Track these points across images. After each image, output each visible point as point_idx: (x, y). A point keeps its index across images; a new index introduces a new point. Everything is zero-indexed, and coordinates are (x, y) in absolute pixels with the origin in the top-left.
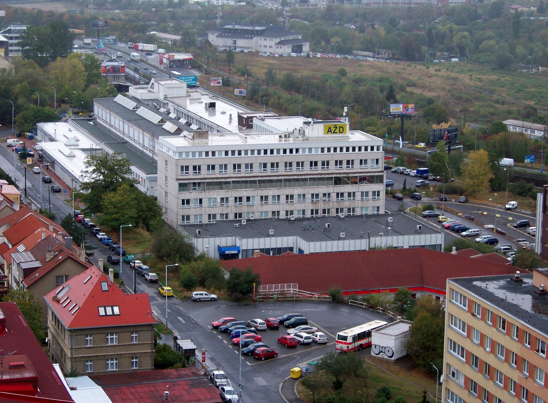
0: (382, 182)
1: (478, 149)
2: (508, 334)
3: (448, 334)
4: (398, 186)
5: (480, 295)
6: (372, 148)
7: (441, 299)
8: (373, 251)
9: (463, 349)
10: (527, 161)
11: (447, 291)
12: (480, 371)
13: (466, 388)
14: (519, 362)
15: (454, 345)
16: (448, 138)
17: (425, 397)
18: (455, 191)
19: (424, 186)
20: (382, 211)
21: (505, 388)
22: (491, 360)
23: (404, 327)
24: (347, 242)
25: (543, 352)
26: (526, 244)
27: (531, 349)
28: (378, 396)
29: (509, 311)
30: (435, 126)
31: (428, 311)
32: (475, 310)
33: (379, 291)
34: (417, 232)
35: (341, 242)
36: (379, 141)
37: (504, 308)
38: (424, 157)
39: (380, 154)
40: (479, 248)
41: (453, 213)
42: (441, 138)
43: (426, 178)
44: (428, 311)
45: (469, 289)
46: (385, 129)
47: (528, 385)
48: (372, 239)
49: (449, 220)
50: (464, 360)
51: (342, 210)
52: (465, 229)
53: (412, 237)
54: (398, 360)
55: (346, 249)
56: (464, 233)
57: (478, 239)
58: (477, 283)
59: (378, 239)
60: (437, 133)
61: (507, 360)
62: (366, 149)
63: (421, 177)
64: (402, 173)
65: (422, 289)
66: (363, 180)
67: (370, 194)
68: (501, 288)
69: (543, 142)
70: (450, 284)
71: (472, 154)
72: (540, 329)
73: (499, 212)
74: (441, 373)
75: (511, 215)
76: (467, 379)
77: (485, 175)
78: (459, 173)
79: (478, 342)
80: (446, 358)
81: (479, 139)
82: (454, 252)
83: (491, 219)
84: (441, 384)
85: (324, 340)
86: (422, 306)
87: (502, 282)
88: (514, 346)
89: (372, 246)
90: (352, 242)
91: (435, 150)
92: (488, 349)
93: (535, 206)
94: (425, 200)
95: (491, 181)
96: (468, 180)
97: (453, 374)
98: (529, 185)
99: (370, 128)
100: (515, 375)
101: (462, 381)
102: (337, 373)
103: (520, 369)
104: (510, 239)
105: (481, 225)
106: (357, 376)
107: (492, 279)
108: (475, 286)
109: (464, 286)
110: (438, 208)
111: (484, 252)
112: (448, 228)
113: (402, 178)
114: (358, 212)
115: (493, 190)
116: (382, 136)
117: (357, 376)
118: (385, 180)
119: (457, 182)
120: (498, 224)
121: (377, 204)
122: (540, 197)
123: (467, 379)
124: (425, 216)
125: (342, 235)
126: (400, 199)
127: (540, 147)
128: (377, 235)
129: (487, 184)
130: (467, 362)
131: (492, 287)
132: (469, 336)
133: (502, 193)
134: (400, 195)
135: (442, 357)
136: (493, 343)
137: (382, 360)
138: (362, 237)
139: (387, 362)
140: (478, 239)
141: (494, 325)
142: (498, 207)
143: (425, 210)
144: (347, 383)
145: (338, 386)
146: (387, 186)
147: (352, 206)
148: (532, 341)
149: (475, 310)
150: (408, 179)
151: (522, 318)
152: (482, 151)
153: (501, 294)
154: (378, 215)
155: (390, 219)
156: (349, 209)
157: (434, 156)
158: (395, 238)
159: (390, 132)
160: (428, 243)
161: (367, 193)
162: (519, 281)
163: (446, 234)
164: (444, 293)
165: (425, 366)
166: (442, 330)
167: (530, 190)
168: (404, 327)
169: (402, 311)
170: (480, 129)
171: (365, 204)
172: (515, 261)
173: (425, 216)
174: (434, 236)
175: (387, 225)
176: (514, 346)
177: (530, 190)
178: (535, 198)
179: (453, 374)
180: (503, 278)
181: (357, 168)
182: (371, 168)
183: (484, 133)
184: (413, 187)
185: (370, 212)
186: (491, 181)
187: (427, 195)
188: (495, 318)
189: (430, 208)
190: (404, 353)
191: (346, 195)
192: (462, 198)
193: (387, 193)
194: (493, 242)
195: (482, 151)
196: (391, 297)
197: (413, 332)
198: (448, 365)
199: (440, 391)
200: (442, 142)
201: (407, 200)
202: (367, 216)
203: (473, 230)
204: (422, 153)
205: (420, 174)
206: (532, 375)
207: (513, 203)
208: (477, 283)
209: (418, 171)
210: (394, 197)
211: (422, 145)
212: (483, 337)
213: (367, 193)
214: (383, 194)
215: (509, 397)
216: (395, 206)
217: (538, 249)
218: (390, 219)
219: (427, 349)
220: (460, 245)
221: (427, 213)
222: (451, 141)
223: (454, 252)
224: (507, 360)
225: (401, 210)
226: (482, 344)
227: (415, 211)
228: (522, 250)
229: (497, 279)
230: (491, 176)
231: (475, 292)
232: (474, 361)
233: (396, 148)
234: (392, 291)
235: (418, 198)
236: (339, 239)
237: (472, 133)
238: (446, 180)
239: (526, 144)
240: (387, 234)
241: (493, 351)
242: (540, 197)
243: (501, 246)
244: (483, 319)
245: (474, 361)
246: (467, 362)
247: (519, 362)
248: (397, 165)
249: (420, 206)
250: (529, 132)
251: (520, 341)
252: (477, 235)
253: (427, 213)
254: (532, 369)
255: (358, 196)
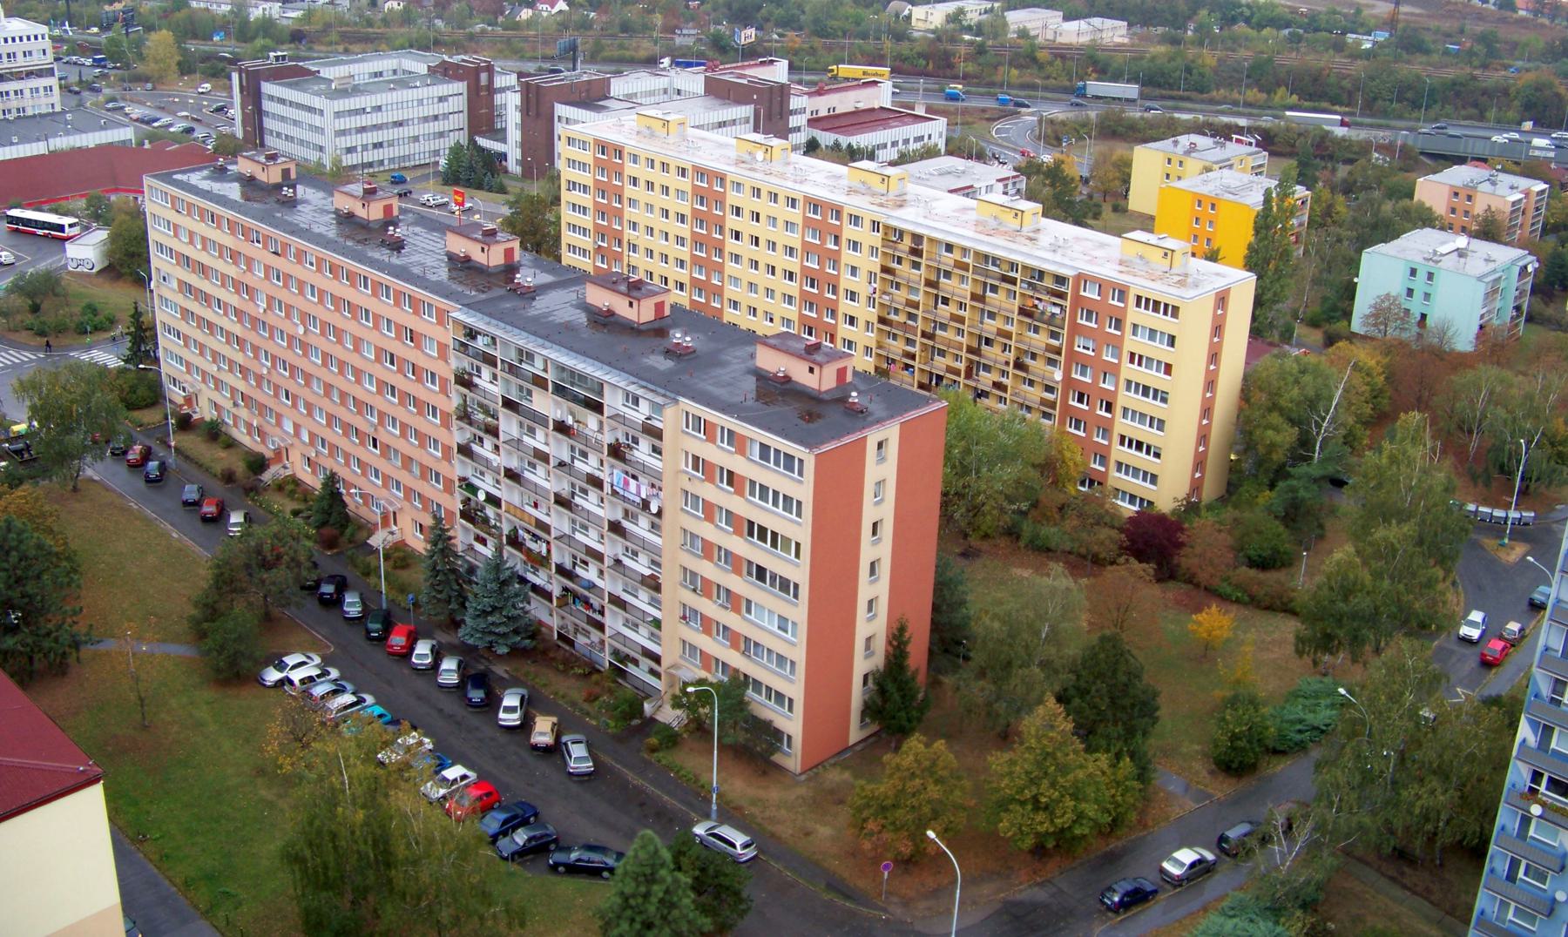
0: (53, 75)
1: (160, 29)
2: (219, 227)
3: (153, 236)
4: (74, 79)
5: (183, 189)
6: (36, 37)
7: (140, 199)
8: (54, 155)
9: (171, 250)
10: (216, 38)
11: (146, 189)
12: (194, 271)
13: (181, 291)
14: (235, 256)
15: (161, 247)
16: (124, 19)
17: (136, 308)
18: (141, 79)
19: (104, 76)
20: (58, 109)
21: (223, 285)
22: (204, 258)
23: (102, 235)
24: (21, 147)
25: (258, 242)
26: (225, 130)
27: (246, 240)
28: (83, 314)
29: (217, 203)
30: (107, 8)
31: (127, 213)
32: (179, 206)
33: (67, 198)
34: (103, 128)
35: (14, 148)
36: (44, 29)
37: (211, 201)
38: (100, 44)
39: (47, 44)
40: (174, 138)
41: (142, 103)
42: (116, 20)
43: (105, 67)
44: (127, 213)
45: (169, 183)
46: (48, 15)
47: (248, 279)
48: (51, 141)
49: (136, 111)
50: (174, 261)
51: (9, 111)
52: (156, 120)
53: (97, 134)
54: (100, 272)
55: (22, 155)
56: (156, 124)
57: (172, 130)
58: (178, 177)
59: (58, 139)
60: (111, 15)
61: (221, 256)
62: (29, 38)
63: (98, 67)
64: (75, 63)
65: (116, 190)
66: (30, 74)
67: (41, 90)
68: (205, 178)
69: (231, 18)
70: (147, 181)
71: (154, 36)
72: (253, 218)
73: (192, 98)
74: (150, 279)
75: (206, 100)
76: (180, 282)
77: (171, 58)
78: (141, 57)
79: (187, 240)
80: (154, 263)
81: (160, 18)
82: (147, 146)
83: (184, 106)
84: (151, 291)
85: (11, 259)
86: (120, 210)
87: (205, 173)
88: (227, 240)
89: (52, 148)
90: (27, 146)
91: (111, 34)
92: (199, 247)
93: (231, 88)
94: (107, 91)
95: (179, 64)
96: (152, 65)
97: (164, 279)
98: (221, 65)
99: (31, 14)
100: (232, 271)
101: (175, 285)
102: (30, 295)
103: (236, 263)
104: (208, 125)
105: (174, 113)
106: (56, 295)
107: (193, 170)
108: (175, 180)
109: (163, 181)
110: (124, 99)
111: (180, 143)
112: (137, 120)
113: (76, 69)
114: (30, 112)
115: (183, 74)
116: (47, 23)
117: (56, 295)
118: (56, 73)
119: (140, 68)
120: (192, 110)
121: (51, 100)
122: (235, 76)
123: (180, 282)
124: (109, 110)
125: (15, 139)
126: (77, 93)
127: (229, 22)
128: (55, 135)
129: (175, 68)
130: (178, 264)
131: (195, 178)
132: (176, 235)
133: (193, 77)
134: (77, 89)
135: (149, 262)
136: (204, 239)
137: (82, 275)
138: (38, 140)
139: (88, 275)
140: (172, 130)
141: (202, 220)
142: (190, 92)
143: (107, 103)
144: (45, 306)
145: (35, 309)
146: (60, 79)
147: (20, 106)
148: (246, 232)
149: (179, 206)
150: (84, 70)
151: (232, 209)
152: (164, 32)
153: (206, 185)
154: (54, 114)
155: (69, 117)
156: (18, 110)
157: (111, 41)
158: (77, 137)
159: (55, 18)
160: (116, 139)
161: (37, 90)
162: (223, 170)
163: (135, 127)
164: (143, 192)
165: (131, 274)
166: (146, 232)
167: (223, 70)
168: (102, 235)
169: (97, 217)
170: (160, 8)
171: (37, 102)
172: (216, 149)
173: (109, 110)
174: (122, 130)
175: (67, 122)
176: (227, 240)
177: (223, 70)
178: (230, 78)
179: (164, 279)
180: (205, 168)
181: (20, 61)
182: (38, 61)
183: (165, 11)
184: (90, 78)
185: (44, 111)
186: (179, 64)
187: (108, 86)
188: (202, 212)
189: (113, 100)
190: (106, 264)
191: (12, 93)
192: (149, 86)
193: (61, 87)
194: (190, 131)
195: (164, 32)
196: (82, 203)
197: (113, 238)
198: (158, 270)
199: (152, 299)
200: (118, 25)
201: (86, 94)
202: (41, 115)
203: (166, 120)
204: (96, 38)
205: (98, 63)
206: (250, 269)
207: (208, 86)
208: (178, 177)
209: (94, 60)
210: (70, 91)
211: (95, 30)
212: (191, 234)
213: (37, 90)
214: (56, 89)
215: (227, 294)
216: (74, 100)
217: (240, 134)
218: (69, 117)
219: (132, 255)
220: (152, 138)
221: (110, 105)
222: (128, 23)
223: (147, 146)
224: (221, 256)
225: (81, 104)
226: (191, 242)
227: (96, 104)
228: (221, 136)
229: (200, 169)
230: (178, 58)
231: (177, 187)
232: (186, 261)
233: (65, 36)
234: (82, 196)
235: (98, 91)
236: (12, 144)
237: (152, 12)
238: (127, 66)
239: (214, 21)
240: (67, 133)
241: (204, 248)
242: (235, 76)
243: (200, 133)
244: (189, 214)
245: (186, 261)
246: (178, 264)
247: (235, 256)
248: (68, 55)
249: (101, 98)
250: (215, 7)
251: (233, 233)
252: (171, 125)
253: (110, 105)
254: (250, 262)
255: (27, 93)
